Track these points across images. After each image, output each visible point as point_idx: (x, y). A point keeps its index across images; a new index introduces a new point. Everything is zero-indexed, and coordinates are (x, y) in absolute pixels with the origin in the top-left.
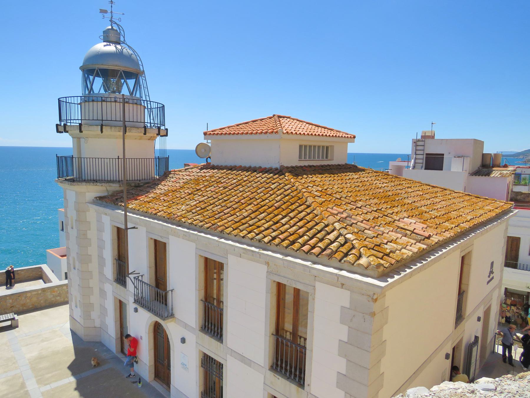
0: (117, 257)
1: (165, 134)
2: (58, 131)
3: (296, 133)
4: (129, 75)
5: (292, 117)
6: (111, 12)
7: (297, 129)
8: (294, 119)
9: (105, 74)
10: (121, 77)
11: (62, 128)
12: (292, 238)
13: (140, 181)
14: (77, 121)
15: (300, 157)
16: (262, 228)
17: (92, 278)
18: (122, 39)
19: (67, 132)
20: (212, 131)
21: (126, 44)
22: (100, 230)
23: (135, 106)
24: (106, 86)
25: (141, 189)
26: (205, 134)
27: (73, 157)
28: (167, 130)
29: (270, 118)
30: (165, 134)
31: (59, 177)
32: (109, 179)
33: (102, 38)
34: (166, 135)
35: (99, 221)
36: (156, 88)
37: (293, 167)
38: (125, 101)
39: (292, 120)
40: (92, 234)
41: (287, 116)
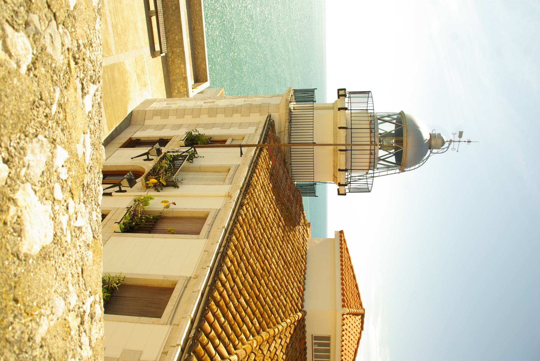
0: (213, 139)
1: (340, 193)
2: (339, 90)
3: (343, 331)
4: (399, 156)
5: (363, 332)
6: (459, 141)
7: (349, 334)
8: (360, 333)
9: (399, 134)
10: (396, 148)
11: (342, 94)
12: (222, 303)
13: (290, 164)
14: (349, 107)
15: (316, 338)
16: (235, 275)
17: (193, 117)
18: (434, 151)
19: (339, 98)
20: (344, 240)
21: (429, 156)
22: (240, 125)
23: (368, 160)
24: (388, 135)
25: (282, 164)
26: (341, 232)
27: (313, 102)
28: (345, 194)
29: (361, 305)
30: (340, 193)
31: (295, 91)
32: (292, 134)
33: (434, 132)
34: (339, 194)
35: (250, 124)
36: (389, 184)
37: (304, 326)
38: (373, 153)
39: (359, 331)
40: (237, 118)
41: (364, 326)
